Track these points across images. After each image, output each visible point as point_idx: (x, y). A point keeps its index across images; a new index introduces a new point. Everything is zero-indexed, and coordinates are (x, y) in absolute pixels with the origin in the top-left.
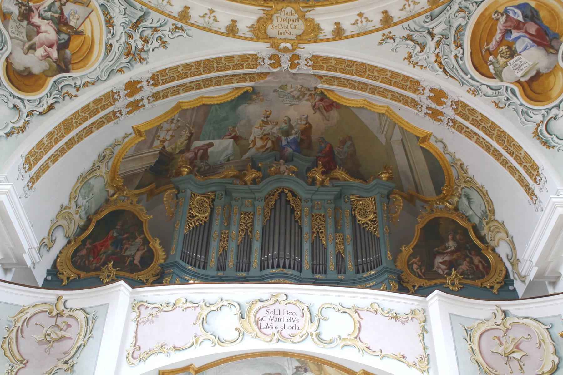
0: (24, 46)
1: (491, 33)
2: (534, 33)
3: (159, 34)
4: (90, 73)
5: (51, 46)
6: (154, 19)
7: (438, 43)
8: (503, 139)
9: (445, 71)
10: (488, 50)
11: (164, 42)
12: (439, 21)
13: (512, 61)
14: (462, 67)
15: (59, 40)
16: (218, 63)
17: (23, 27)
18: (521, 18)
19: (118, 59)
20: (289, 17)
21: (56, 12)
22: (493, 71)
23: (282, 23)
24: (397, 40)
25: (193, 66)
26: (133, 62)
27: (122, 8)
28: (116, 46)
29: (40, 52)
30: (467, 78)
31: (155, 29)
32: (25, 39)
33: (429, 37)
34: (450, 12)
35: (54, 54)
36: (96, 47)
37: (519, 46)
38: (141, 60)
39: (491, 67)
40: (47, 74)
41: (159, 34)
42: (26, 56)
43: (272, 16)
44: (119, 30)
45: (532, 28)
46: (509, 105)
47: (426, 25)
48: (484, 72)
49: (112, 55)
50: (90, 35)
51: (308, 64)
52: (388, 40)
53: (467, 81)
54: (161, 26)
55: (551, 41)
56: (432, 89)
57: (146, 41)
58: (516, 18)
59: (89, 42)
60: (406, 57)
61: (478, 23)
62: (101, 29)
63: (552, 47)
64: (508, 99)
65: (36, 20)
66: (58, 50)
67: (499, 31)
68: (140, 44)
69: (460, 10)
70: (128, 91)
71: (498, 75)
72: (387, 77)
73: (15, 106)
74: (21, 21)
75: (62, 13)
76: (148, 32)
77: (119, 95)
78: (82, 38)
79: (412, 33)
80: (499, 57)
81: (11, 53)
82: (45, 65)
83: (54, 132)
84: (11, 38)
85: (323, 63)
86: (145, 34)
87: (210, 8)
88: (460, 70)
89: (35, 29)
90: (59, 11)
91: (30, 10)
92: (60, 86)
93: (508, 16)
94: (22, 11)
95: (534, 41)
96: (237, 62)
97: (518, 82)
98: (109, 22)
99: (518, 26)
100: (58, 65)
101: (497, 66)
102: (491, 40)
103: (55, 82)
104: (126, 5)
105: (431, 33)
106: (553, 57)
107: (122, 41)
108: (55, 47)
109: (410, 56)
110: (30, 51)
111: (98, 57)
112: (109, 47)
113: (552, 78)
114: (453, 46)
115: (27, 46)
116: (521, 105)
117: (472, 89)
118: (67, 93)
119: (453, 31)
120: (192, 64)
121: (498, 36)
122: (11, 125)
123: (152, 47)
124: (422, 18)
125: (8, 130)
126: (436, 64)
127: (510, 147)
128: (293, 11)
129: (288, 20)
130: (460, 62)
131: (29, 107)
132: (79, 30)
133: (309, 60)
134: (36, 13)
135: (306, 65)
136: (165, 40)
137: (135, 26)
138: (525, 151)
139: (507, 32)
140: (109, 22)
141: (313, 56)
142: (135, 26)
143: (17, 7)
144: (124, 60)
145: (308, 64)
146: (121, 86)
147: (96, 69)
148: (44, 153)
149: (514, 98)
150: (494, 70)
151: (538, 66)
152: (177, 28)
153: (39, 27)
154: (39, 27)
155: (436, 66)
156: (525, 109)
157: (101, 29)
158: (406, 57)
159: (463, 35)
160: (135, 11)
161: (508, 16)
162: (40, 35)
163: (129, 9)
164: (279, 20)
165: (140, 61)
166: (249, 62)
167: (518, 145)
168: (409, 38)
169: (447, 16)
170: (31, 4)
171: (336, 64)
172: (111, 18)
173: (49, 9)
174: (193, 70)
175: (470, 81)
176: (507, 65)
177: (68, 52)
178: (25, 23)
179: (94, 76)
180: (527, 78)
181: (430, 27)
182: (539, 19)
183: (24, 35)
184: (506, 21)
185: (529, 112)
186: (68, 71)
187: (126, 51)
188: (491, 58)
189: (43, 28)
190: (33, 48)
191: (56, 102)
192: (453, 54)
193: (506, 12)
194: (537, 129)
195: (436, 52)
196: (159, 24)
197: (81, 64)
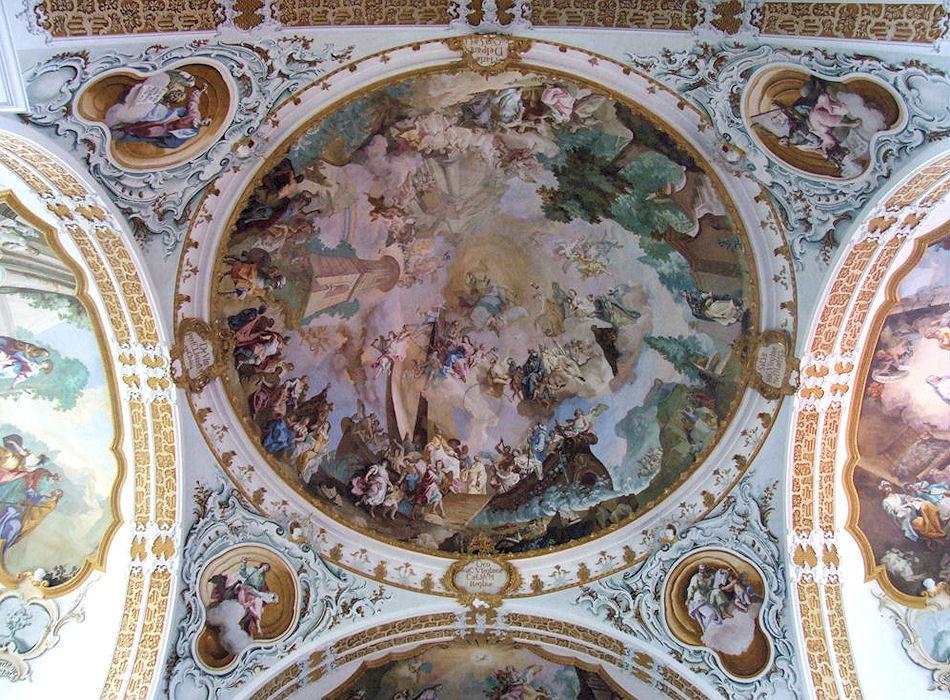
0: (858, 127)
1: (204, 105)
2: (151, 129)
3: (670, 67)
4: (784, 61)
5: (822, 109)
6: (675, 84)
7: (271, 69)
8: (126, 18)
9: (251, 47)
10: (200, 90)
11: (666, 56)
12: (277, 91)
13: (164, 93)
14: (228, 60)
15: (809, 111)
16: (591, 15)
17: (847, 143)
18: (175, 133)
19: (738, 59)
20: (485, 55)
21: (798, 135)
22: (183, 73)
23: (494, 47)
24: (329, 56)
25: (631, 21)
26: (717, 48)
27: (713, 105)
28: (736, 73)
29: (840, 111)
30: (216, 53)
31: (674, 73)
32: (851, 131)
33: (284, 72)
34: (267, 103)
35: (822, 100)
36: (764, 80)
37: (163, 109)
38: (706, 47)
39: (187, 75)
40: (847, 88)
41: (670, 67)
42: (860, 117)
43: (508, 57)
44: (725, 87)
45: (155, 132)
46: (142, 56)
47: (294, 81)
48: (194, 68)
49: (745, 67)
50: (766, 97)
51: (454, 7)
52: (341, 54)
53: (213, 49)
54: (666, 74)
55: (126, 133)
56: (262, 22)
57: (691, 65)
58: (181, 130)
59: (773, 92)
60: (310, 44)
61: (226, 106)
62: (748, 97)
63: (120, 130)
64: (147, 60)
65: (827, 141)
66: (816, 101)
67: (196, 110)
68: (701, 63)
69: (254, 110)
70: (736, 17)
71: (173, 74)
72: (331, 11)
73: (910, 87)
74: (847, 149)
75: (792, 132)
76: (686, 72)
77: (754, 17)
78: (778, 98)
79: (311, 68)
80: (182, 89)
81: (879, 130)
82: (841, 97)
83: (872, 31)
84: (869, 142)
85: (432, 11)
86: (691, 72)
87: (595, 66)
88: (230, 55)
89: (834, 134)
90: (794, 134)
91: (829, 152)
92: (833, 68)
93: (192, 127)
94: (839, 156)
95: (147, 122)
96: (563, 12)
97: (142, 81)
98: (735, 99)
99: (175, 125)
100: (825, 89)
101: (181, 80)
102: (201, 99)
103: (838, 75)
104: (708, 107)
105: (281, 74)
106: (112, 123)
107: (724, 75)
108: (818, 106)
109: (304, 45)
110: (852, 118)
111: (763, 73)
112: (746, 75)
113: (101, 107)
114: (249, 74)
115: (854, 125)
116: (124, 66)
117: (202, 46)
118: (826, 58)
119: (255, 88)
120: (629, 23)
121: (194, 106)
122: (929, 77)
123: (685, 56)
124: (300, 88)
125: (936, 77)
126: (265, 49)
127: (111, 12)
128: (479, 63)
129: (486, 51)
130: (233, 64)
131: (892, 75)
132: (775, 107)
133: (455, 14)
134: (824, 145)
135: (458, 6)
136: (665, 59)
137: (701, 83)
138: (86, 34)
139: (185, 114)
140: (735, 99)
141: (448, 22)
142: (701, 83)
143: (843, 162)
144: (730, 54)
145: (454, 7)
146: (744, 33)
147: (773, 62)
148: (905, 10)
149: (138, 66)
150: (182, 76)
151: (126, 106)
152: (645, 67)
153: (827, 133)
154: (827, 133)
155: (264, 47)
156: (117, 64)
157: (748, 97)
158: (310, 44)
159: (240, 89)
160: (696, 97)
161: (192, 127)
162: (830, 125)
163: (704, 101)
164: (499, 51)
165: (707, 46)
166: (544, 10)
167: (102, 31)
168: (312, 63)
169: (268, 99)
170: (826, 157)
171: (412, 11)
172: (731, 102)
173: (806, 141)
174: (632, 11)
175: (210, 52)
176: (168, 87)
177: (804, 93)
178: (842, 145)
179: (779, 55)
180: (133, 90)
181: (287, 82)
182: (153, 143)
183: (850, 136)
184: (191, 122)
185: (108, 65)
186: (813, 77)
187: (723, 63)
188: (193, 84)
189: (824, 130)
190: (847, 119)
191: (848, 58)
192: (245, 68)
193: (196, 130)
194: (86, 60)
195: (270, 62)
196: (668, 76)
197: (791, 75)
